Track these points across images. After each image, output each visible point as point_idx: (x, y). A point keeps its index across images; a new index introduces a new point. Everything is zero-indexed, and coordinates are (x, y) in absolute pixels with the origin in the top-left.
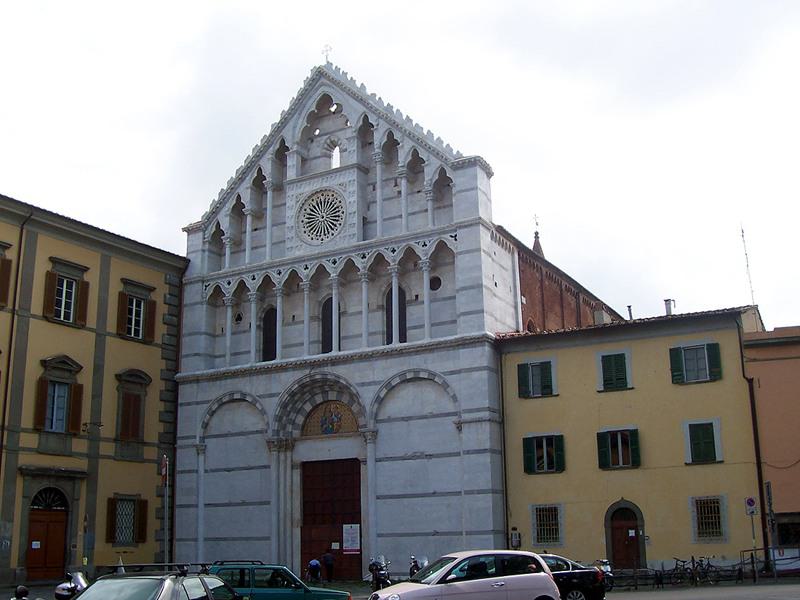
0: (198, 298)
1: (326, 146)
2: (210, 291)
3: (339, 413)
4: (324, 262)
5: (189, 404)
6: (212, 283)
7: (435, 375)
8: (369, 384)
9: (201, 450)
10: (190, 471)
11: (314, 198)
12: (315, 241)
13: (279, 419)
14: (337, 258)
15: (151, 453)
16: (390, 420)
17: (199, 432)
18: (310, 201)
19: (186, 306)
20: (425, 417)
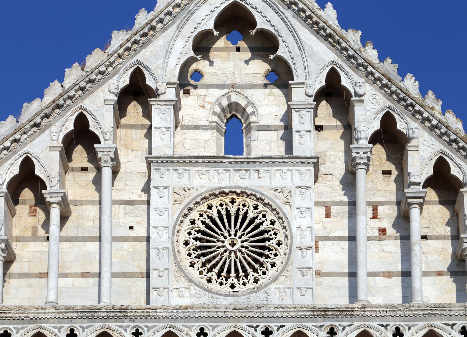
1: (218, 110)
11: (215, 202)
12: (214, 286)
14: (273, 326)
18: (204, 207)
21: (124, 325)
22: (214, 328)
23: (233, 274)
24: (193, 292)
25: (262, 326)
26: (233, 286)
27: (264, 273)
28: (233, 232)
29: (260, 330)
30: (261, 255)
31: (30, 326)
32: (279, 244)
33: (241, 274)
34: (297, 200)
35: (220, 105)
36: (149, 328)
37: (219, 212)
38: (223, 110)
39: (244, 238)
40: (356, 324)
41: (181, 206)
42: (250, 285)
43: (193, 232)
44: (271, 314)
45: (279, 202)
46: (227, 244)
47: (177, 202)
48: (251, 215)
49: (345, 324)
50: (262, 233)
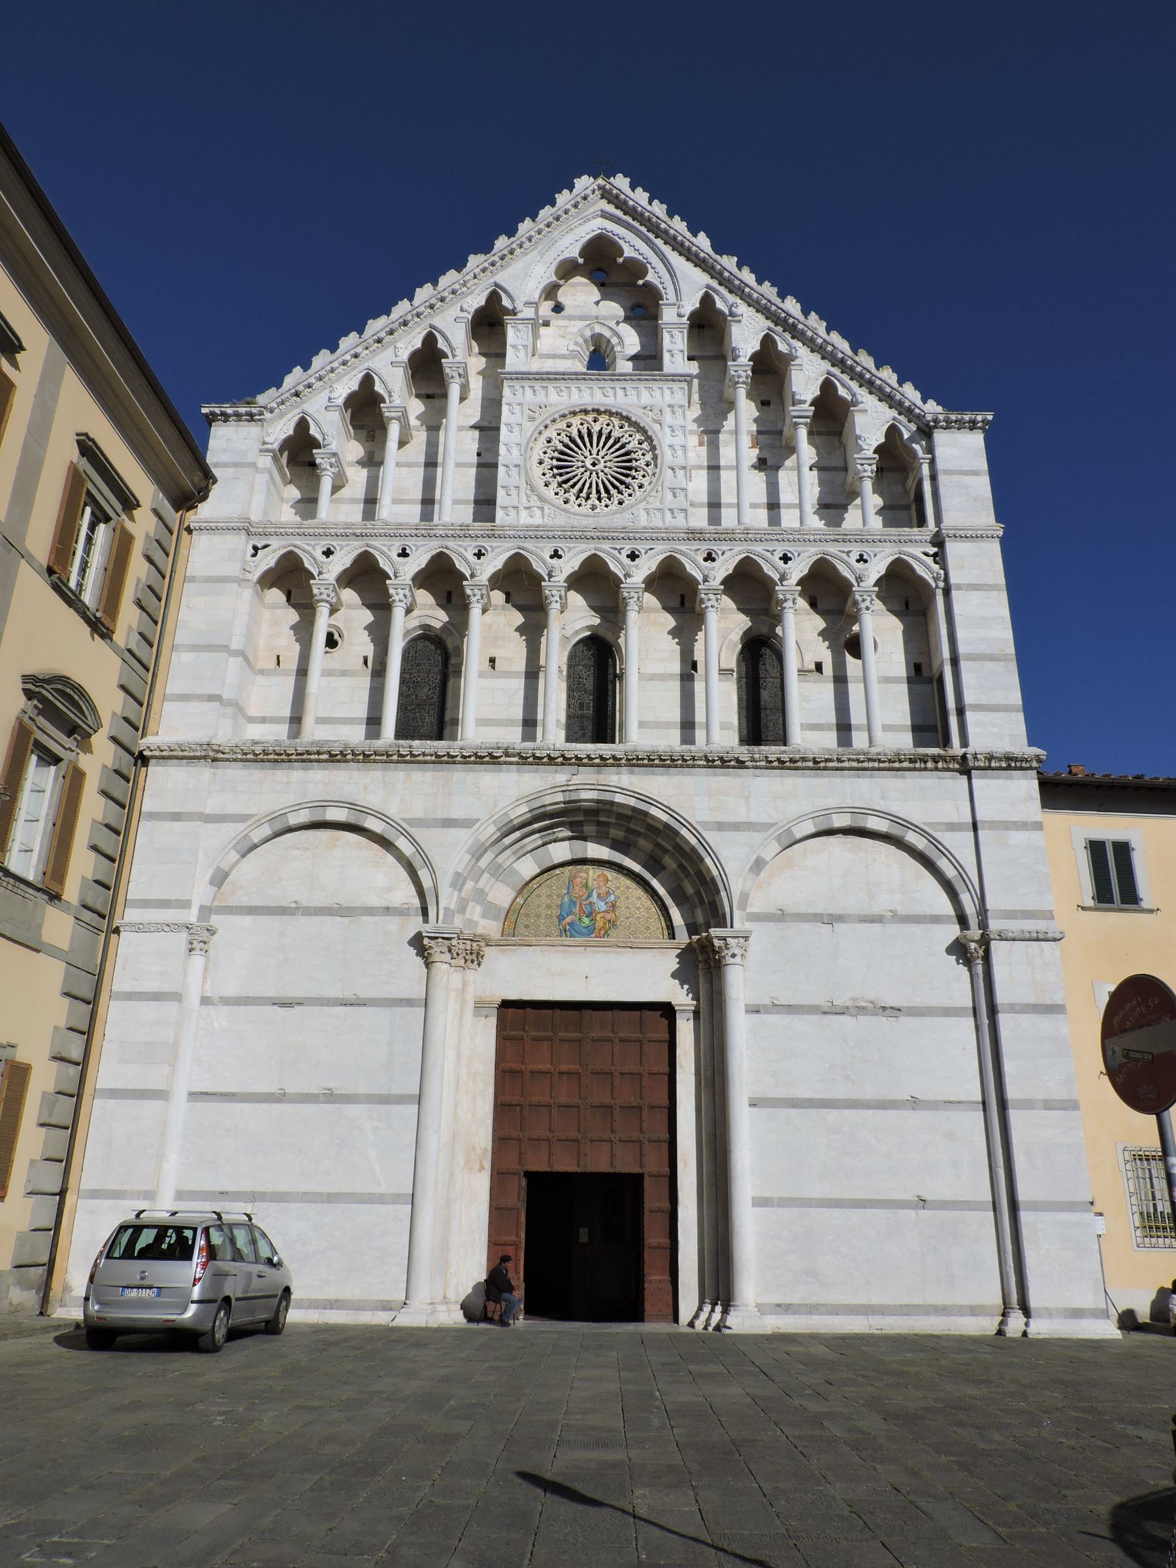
0: (234, 569)
1: (580, 340)
2: (267, 560)
3: (608, 894)
4: (605, 550)
5: (176, 817)
6: (275, 543)
7: (908, 825)
8: (736, 827)
9: (199, 938)
10: (156, 997)
11: (576, 421)
12: (573, 506)
13: (458, 881)
14: (640, 547)
15: (58, 926)
16: (781, 916)
17: (201, 893)
19: (192, 579)
20: (877, 919)
21: (465, 544)
22: (570, 549)
23: (594, 495)
24: (546, 512)
25: (628, 548)
26: (593, 508)
27: (630, 495)
28: (594, 451)
29: (625, 552)
30: (627, 476)
31: (357, 543)
32: (647, 465)
33: (604, 495)
34: (668, 418)
35: (582, 335)
36: (493, 549)
37: (579, 431)
38: (585, 341)
39: (607, 458)
40: (737, 549)
41: (536, 423)
42: (614, 506)
43: (549, 451)
44: (638, 536)
45: (649, 420)
46: (588, 463)
47: (532, 419)
48: (616, 433)
49: (725, 548)
50: (628, 453)
